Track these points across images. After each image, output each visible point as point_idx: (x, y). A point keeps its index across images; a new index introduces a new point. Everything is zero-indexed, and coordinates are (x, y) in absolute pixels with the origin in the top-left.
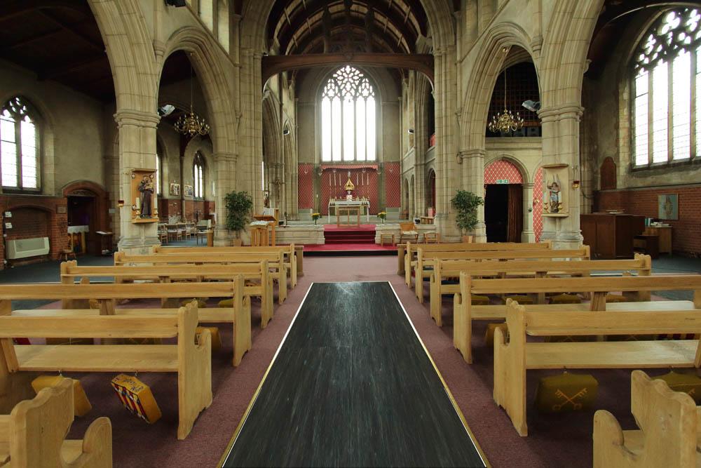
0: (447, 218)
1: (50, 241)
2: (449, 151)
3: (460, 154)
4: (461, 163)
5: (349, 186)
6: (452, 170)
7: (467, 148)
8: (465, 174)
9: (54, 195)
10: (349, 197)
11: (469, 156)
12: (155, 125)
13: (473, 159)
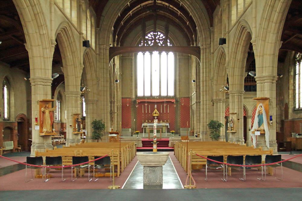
0: (206, 134)
1: (14, 143)
2: (207, 99)
3: (212, 101)
4: (213, 105)
5: (156, 113)
6: (209, 109)
7: (216, 98)
8: (215, 111)
9: (14, 121)
10: (156, 121)
11: (217, 102)
12: (50, 84)
13: (219, 104)
